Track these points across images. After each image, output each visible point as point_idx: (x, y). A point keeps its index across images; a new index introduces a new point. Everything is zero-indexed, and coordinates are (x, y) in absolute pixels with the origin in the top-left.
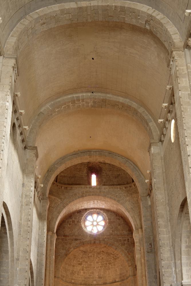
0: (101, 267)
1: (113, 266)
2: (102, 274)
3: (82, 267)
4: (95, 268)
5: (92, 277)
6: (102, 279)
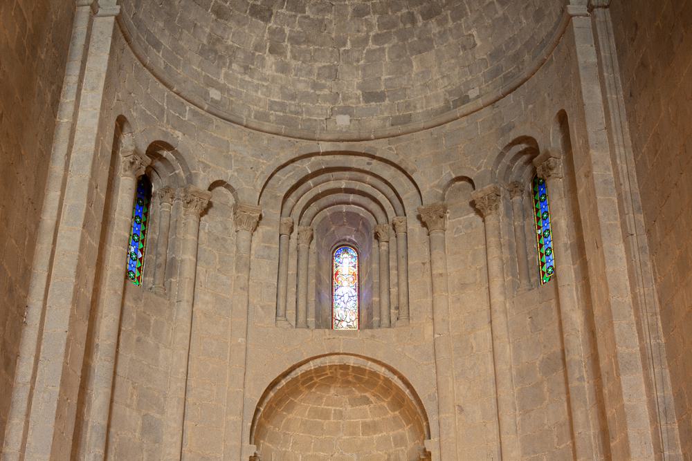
0: (377, 38)
1: (451, 24)
2: (383, 78)
3: (273, 32)
4: (344, 44)
5: (326, 91)
6: (387, 102)
